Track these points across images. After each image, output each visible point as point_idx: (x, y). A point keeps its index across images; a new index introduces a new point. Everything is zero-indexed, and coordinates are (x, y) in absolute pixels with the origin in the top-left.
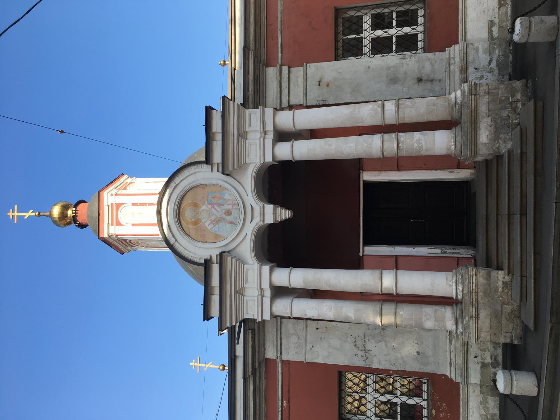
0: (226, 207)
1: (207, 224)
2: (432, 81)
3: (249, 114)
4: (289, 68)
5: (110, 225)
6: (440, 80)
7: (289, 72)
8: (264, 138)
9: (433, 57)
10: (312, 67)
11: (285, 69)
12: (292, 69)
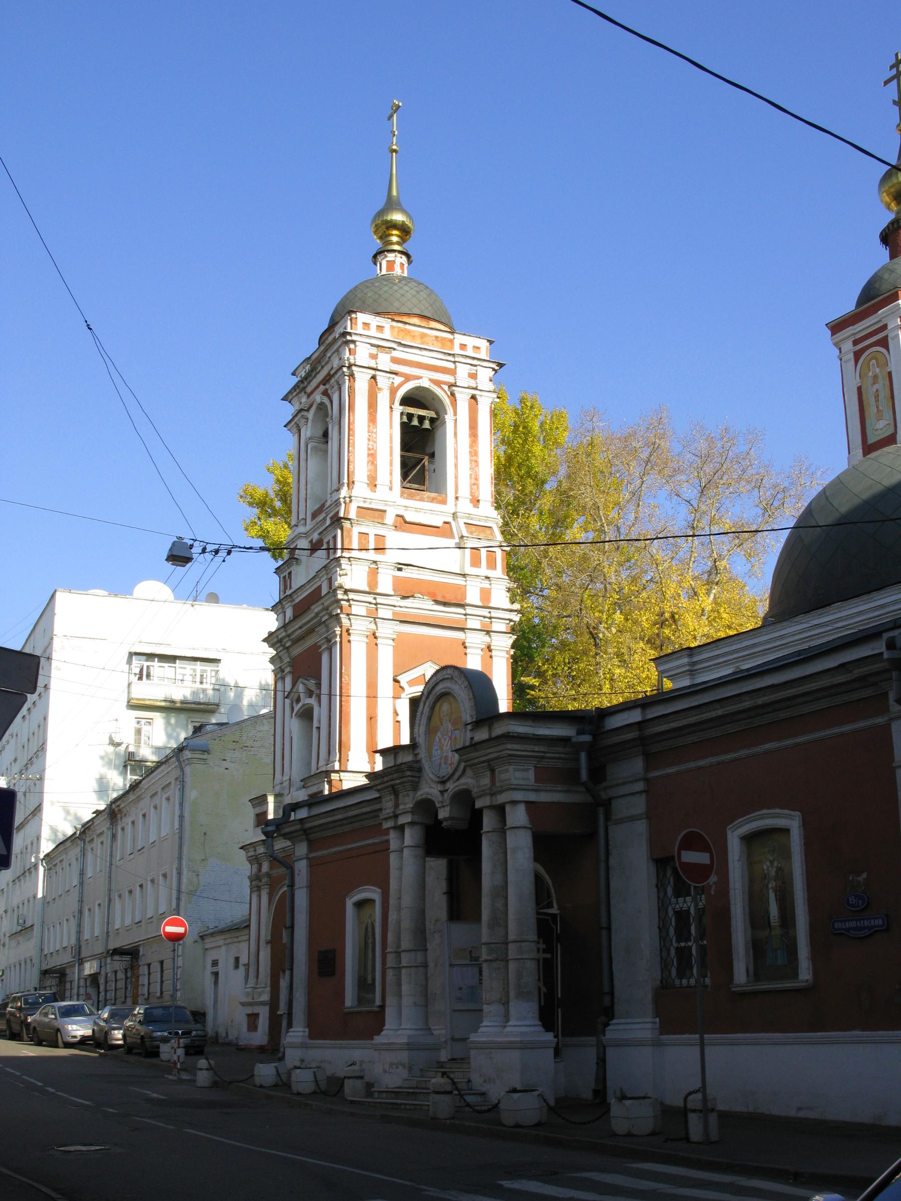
1: (439, 734)
4: (645, 791)
5: (853, 339)
7: (640, 792)
8: (492, 795)
10: (641, 827)
11: (640, 786)
12: (644, 795)
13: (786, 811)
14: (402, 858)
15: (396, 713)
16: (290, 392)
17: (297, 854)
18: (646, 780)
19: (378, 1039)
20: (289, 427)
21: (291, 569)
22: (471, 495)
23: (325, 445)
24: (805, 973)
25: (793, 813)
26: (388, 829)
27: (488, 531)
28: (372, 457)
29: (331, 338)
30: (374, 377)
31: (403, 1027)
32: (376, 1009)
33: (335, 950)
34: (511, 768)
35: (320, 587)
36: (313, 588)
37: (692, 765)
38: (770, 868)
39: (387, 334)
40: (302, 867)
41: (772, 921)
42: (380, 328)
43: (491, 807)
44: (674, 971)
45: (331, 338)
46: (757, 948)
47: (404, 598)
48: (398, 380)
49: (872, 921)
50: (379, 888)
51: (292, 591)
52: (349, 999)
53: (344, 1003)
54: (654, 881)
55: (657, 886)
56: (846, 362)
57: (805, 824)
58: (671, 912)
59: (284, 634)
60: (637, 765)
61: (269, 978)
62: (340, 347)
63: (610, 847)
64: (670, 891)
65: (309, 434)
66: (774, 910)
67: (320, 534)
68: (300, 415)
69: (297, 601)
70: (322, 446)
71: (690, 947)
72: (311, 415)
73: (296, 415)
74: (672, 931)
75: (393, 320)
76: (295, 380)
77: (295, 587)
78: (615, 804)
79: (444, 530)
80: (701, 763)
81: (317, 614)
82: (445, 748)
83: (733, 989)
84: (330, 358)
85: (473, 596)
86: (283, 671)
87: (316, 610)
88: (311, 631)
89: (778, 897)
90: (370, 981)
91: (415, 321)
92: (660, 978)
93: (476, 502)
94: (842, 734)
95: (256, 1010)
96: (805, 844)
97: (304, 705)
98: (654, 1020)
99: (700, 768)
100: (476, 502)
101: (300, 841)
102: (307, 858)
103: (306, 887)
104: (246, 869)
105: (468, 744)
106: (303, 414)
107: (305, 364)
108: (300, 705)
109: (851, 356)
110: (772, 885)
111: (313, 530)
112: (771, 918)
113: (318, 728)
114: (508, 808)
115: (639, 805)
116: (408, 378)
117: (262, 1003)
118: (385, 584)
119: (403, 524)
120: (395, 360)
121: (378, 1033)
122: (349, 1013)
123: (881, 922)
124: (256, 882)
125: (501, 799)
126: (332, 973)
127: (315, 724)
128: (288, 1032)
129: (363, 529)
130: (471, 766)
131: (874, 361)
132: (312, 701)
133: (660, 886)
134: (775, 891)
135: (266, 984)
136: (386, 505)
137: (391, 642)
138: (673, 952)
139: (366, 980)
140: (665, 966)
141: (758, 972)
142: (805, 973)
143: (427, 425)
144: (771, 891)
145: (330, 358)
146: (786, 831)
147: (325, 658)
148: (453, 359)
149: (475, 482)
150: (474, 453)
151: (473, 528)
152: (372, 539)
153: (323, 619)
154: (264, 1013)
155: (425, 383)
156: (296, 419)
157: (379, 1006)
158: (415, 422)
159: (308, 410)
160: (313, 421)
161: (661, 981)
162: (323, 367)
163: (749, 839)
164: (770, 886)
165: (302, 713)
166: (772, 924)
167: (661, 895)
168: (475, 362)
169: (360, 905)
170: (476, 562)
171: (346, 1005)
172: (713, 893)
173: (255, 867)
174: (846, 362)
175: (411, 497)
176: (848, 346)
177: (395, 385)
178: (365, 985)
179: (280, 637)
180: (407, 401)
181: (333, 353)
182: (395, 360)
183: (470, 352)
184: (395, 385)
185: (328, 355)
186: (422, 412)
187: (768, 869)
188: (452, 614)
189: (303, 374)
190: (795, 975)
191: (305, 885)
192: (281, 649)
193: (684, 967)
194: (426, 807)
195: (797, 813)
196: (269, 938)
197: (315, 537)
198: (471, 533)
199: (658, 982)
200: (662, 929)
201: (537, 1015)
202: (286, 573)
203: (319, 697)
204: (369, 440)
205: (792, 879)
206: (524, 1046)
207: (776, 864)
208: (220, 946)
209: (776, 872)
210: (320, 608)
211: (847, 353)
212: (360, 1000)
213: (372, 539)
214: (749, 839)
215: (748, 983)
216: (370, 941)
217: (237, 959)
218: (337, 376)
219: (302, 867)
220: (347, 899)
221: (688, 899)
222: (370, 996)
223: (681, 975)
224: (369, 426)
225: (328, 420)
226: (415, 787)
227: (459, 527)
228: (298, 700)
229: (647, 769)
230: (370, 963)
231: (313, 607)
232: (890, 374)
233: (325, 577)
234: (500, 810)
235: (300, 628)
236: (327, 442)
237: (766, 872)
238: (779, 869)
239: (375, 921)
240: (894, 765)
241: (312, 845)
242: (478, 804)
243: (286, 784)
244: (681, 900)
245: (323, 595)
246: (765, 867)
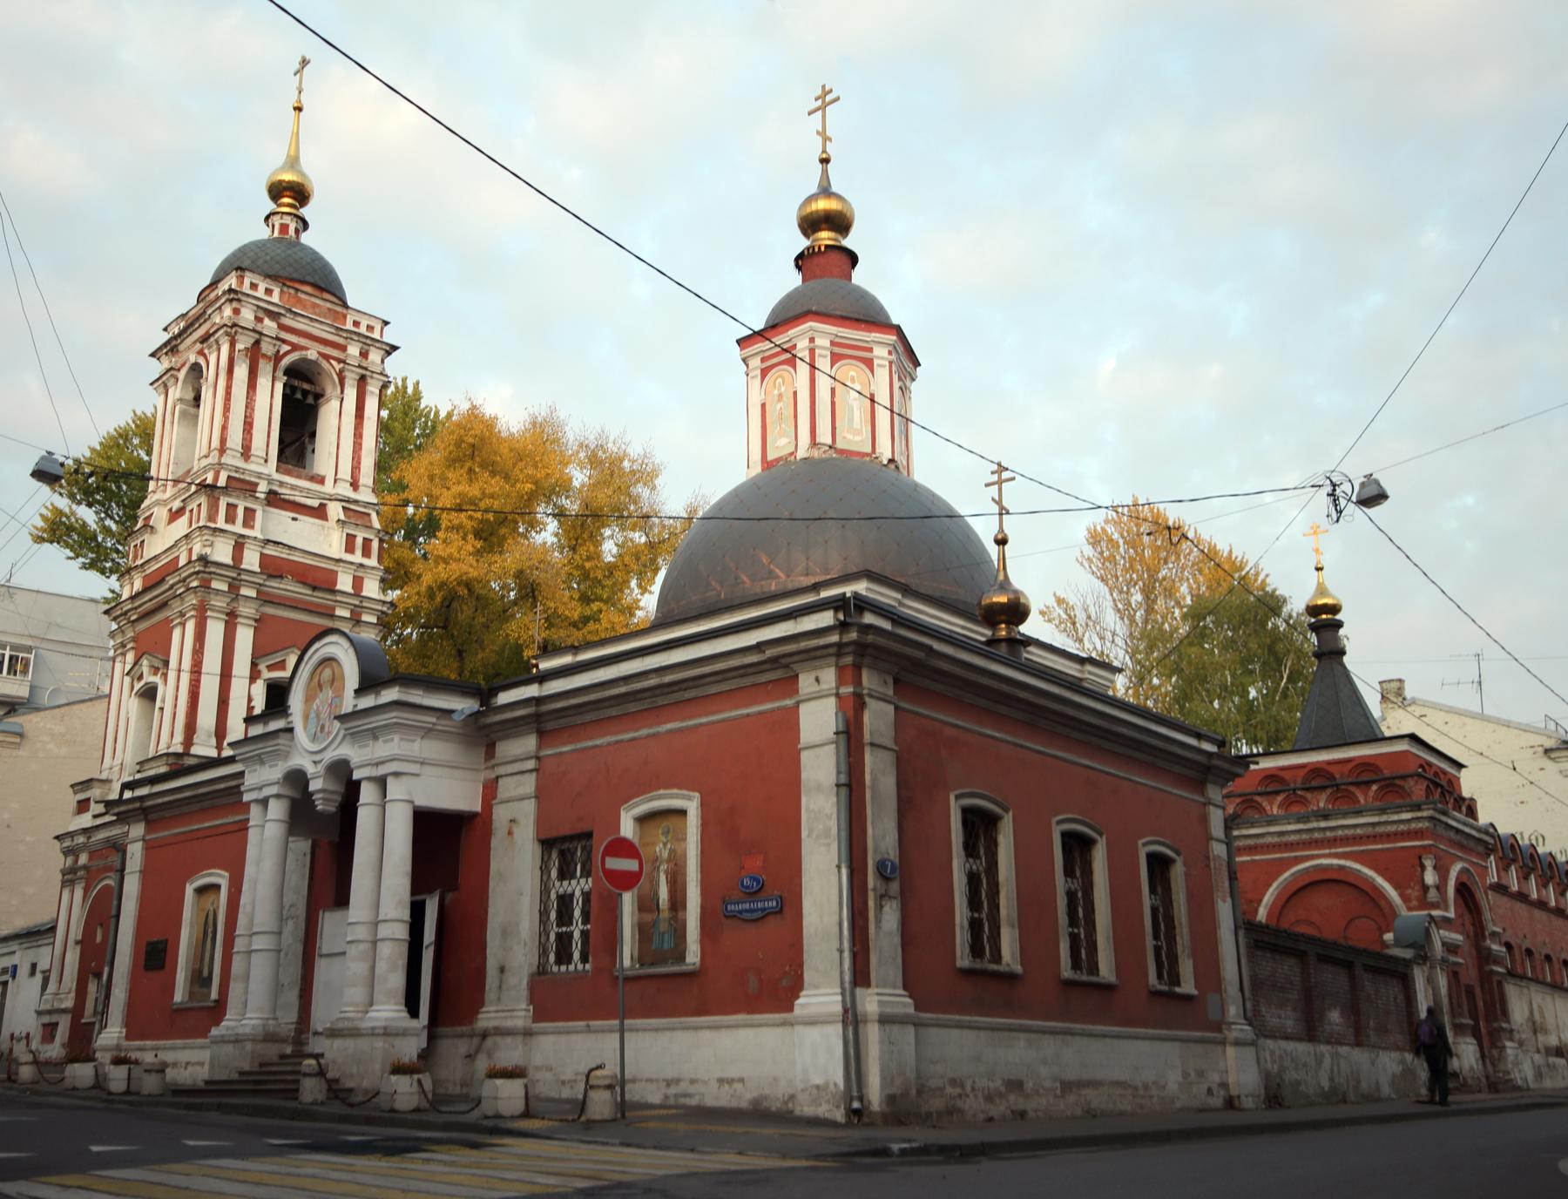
0: (327, 724)
1: (317, 701)
2: (500, 987)
3: (392, 739)
6: (499, 999)
7: (531, 771)
8: (373, 765)
10: (530, 807)
11: (531, 764)
13: (685, 792)
14: (262, 834)
15: (250, 699)
16: (160, 349)
17: (130, 835)
18: (538, 758)
19: (214, 1031)
20: (156, 385)
21: (146, 537)
22: (352, 478)
23: (195, 410)
24: (693, 955)
25: (691, 794)
26: (248, 804)
27: (366, 518)
28: (248, 425)
29: (213, 295)
30: (257, 342)
31: (247, 1016)
32: (212, 1004)
33: (167, 940)
34: (396, 737)
35: (177, 558)
36: (169, 559)
37: (590, 743)
39: (275, 298)
40: (135, 852)
42: (268, 291)
43: (369, 779)
44: (552, 958)
45: (213, 295)
46: (644, 932)
47: (271, 576)
48: (286, 348)
50: (227, 871)
51: (142, 561)
52: (178, 997)
53: (172, 997)
55: (541, 868)
56: (753, 378)
57: (702, 804)
58: (553, 896)
59: (130, 606)
60: (529, 743)
61: (75, 983)
62: (223, 304)
64: (554, 873)
65: (178, 395)
66: (663, 893)
67: (183, 501)
68: (169, 375)
69: (148, 572)
70: (193, 410)
71: (572, 932)
72: (182, 375)
73: (164, 374)
74: (553, 915)
75: (284, 284)
76: (166, 337)
77: (146, 557)
78: (501, 781)
79: (320, 512)
80: (598, 742)
81: (172, 587)
82: (322, 716)
84: (210, 315)
85: (345, 583)
86: (124, 646)
87: (171, 582)
88: (164, 605)
90: (205, 973)
91: (308, 289)
93: (355, 485)
94: (748, 715)
95: (54, 1018)
96: (702, 825)
97: (146, 684)
99: (596, 747)
100: (355, 485)
101: (139, 821)
102: (144, 840)
103: (140, 872)
104: (59, 862)
105: (350, 710)
106: (172, 372)
107: (179, 320)
108: (142, 683)
109: (758, 372)
110: (663, 867)
111: (174, 497)
113: (162, 709)
114: (390, 781)
115: (528, 784)
116: (295, 347)
117: (64, 1011)
118: (251, 560)
119: (274, 499)
120: (282, 327)
121: (217, 1023)
122: (177, 1010)
123: (775, 903)
124: (69, 877)
125: (382, 770)
126: (161, 967)
127: (158, 704)
128: (100, 1033)
129: (232, 501)
130: (352, 734)
131: (780, 380)
132: (157, 679)
133: (544, 869)
134: (666, 872)
135: (70, 990)
136: (260, 478)
137: (253, 623)
138: (552, 937)
139: (201, 972)
140: (543, 952)
141: (642, 958)
142: (693, 955)
143: (310, 400)
145: (210, 315)
146: (682, 813)
147: (177, 633)
148: (345, 335)
149: (356, 467)
150: (358, 434)
151: (352, 514)
152: (240, 512)
153: (178, 592)
154: (64, 1024)
155: (312, 355)
156: (164, 378)
157: (215, 1001)
158: (299, 396)
159: (179, 370)
160: (184, 382)
161: (538, 967)
162: (200, 325)
163: (643, 820)
164: (662, 867)
165: (144, 692)
167: (545, 878)
168: (368, 342)
169: (201, 891)
170: (350, 548)
171: (175, 999)
173: (70, 860)
174: (753, 378)
175: (288, 473)
176: (755, 363)
177: (281, 353)
178: (200, 979)
179: (124, 609)
180: (291, 372)
181: (214, 312)
182: (282, 327)
183: (363, 330)
184: (281, 353)
185: (209, 312)
186: (306, 386)
187: (660, 851)
188: (320, 598)
189: (176, 331)
190: (681, 957)
191: (138, 869)
192: (125, 622)
193: (564, 956)
194: (297, 779)
195: (697, 795)
196: (80, 938)
197: (177, 505)
198: (349, 518)
199: (535, 968)
200: (544, 914)
201: (403, 1001)
202: (139, 542)
203: (165, 676)
204: (247, 407)
205: (685, 862)
206: (387, 1033)
207: (669, 846)
208: (14, 952)
210: (177, 579)
211: (754, 369)
212: (192, 995)
213: (240, 512)
214: (642, 820)
216: (210, 930)
217: (34, 966)
218: (217, 336)
219: (135, 852)
220: (187, 885)
221: (574, 882)
222: (205, 990)
223: (559, 961)
224: (248, 392)
225: (202, 381)
226: (286, 756)
227: (335, 511)
228: (140, 677)
229: (540, 747)
230: (207, 955)
231: (167, 579)
232: (795, 393)
233: (185, 547)
234: (381, 782)
235: (150, 600)
236: (198, 406)
238: (672, 851)
239: (218, 907)
240: (799, 747)
241: (151, 825)
242: (356, 776)
243: (117, 769)
244: (565, 883)
245: (180, 565)
246: (657, 849)
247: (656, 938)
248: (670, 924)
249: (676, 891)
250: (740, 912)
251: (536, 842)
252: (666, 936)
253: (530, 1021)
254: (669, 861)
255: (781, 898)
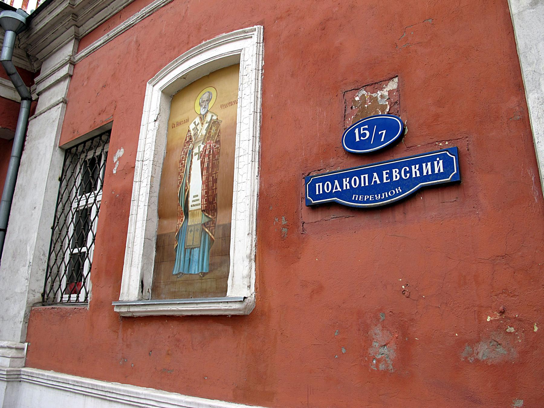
9: (20, 320)
18: (73, 64)
38: (199, 127)
41: (191, 203)
49: (415, 169)
54: (58, 173)
63: (26, 143)
83: (116, 310)
89: (206, 165)
92: (42, 291)
98: (20, 345)
112: (191, 199)
123: (439, 166)
134: (202, 156)
144: (195, 158)
161: (43, 295)
164: (196, 150)
166: (190, 208)
172: (115, 172)
199: (38, 297)
207: (208, 118)
209: (207, 130)
215: (139, 300)
237: (192, 133)
247: (180, 255)
248: (203, 230)
249: (215, 181)
250: (346, 194)
251: (58, 151)
252: (196, 251)
253: (23, 362)
254: (208, 136)
255: (457, 152)
